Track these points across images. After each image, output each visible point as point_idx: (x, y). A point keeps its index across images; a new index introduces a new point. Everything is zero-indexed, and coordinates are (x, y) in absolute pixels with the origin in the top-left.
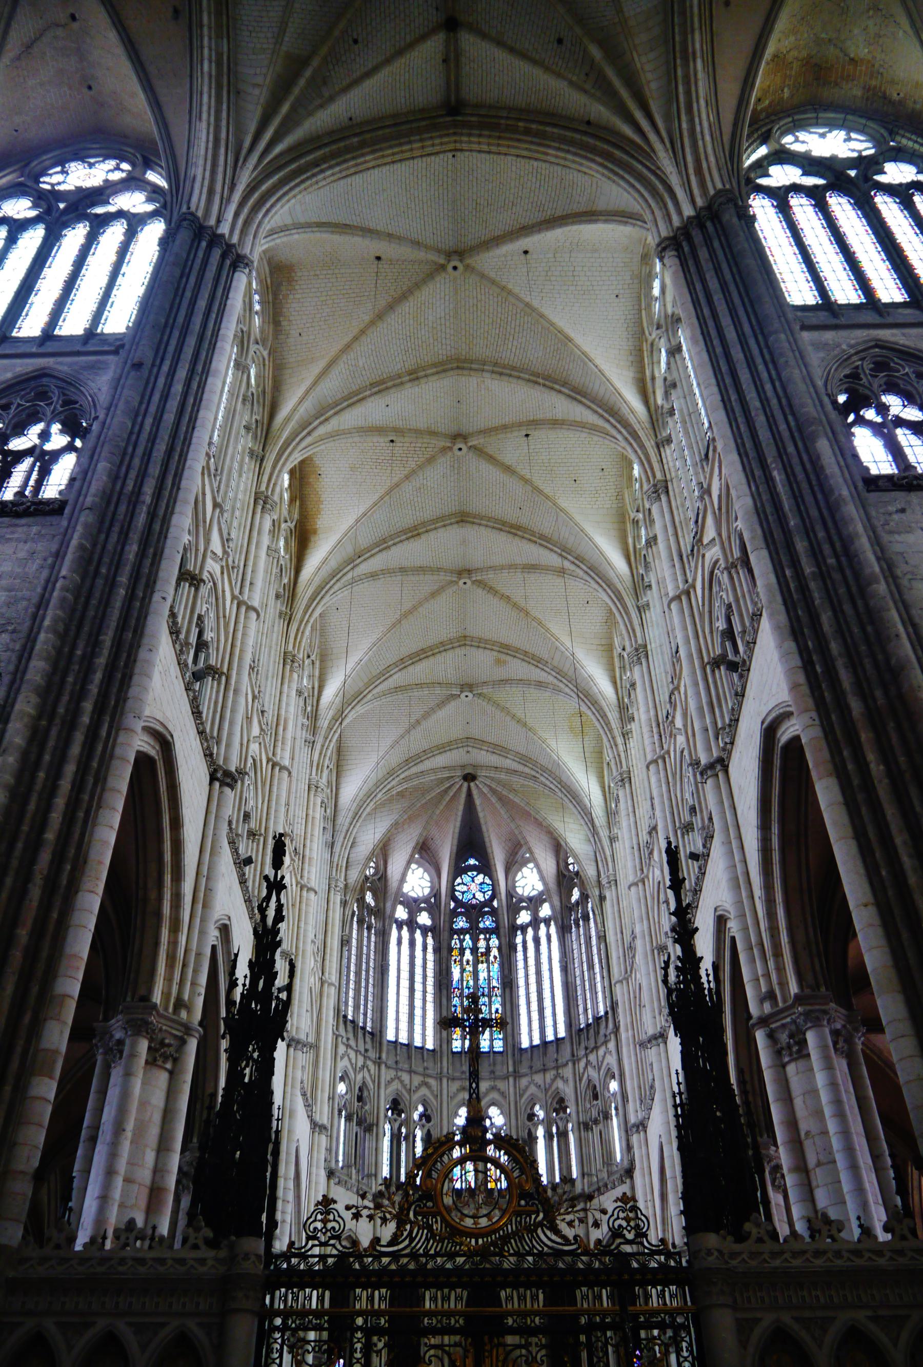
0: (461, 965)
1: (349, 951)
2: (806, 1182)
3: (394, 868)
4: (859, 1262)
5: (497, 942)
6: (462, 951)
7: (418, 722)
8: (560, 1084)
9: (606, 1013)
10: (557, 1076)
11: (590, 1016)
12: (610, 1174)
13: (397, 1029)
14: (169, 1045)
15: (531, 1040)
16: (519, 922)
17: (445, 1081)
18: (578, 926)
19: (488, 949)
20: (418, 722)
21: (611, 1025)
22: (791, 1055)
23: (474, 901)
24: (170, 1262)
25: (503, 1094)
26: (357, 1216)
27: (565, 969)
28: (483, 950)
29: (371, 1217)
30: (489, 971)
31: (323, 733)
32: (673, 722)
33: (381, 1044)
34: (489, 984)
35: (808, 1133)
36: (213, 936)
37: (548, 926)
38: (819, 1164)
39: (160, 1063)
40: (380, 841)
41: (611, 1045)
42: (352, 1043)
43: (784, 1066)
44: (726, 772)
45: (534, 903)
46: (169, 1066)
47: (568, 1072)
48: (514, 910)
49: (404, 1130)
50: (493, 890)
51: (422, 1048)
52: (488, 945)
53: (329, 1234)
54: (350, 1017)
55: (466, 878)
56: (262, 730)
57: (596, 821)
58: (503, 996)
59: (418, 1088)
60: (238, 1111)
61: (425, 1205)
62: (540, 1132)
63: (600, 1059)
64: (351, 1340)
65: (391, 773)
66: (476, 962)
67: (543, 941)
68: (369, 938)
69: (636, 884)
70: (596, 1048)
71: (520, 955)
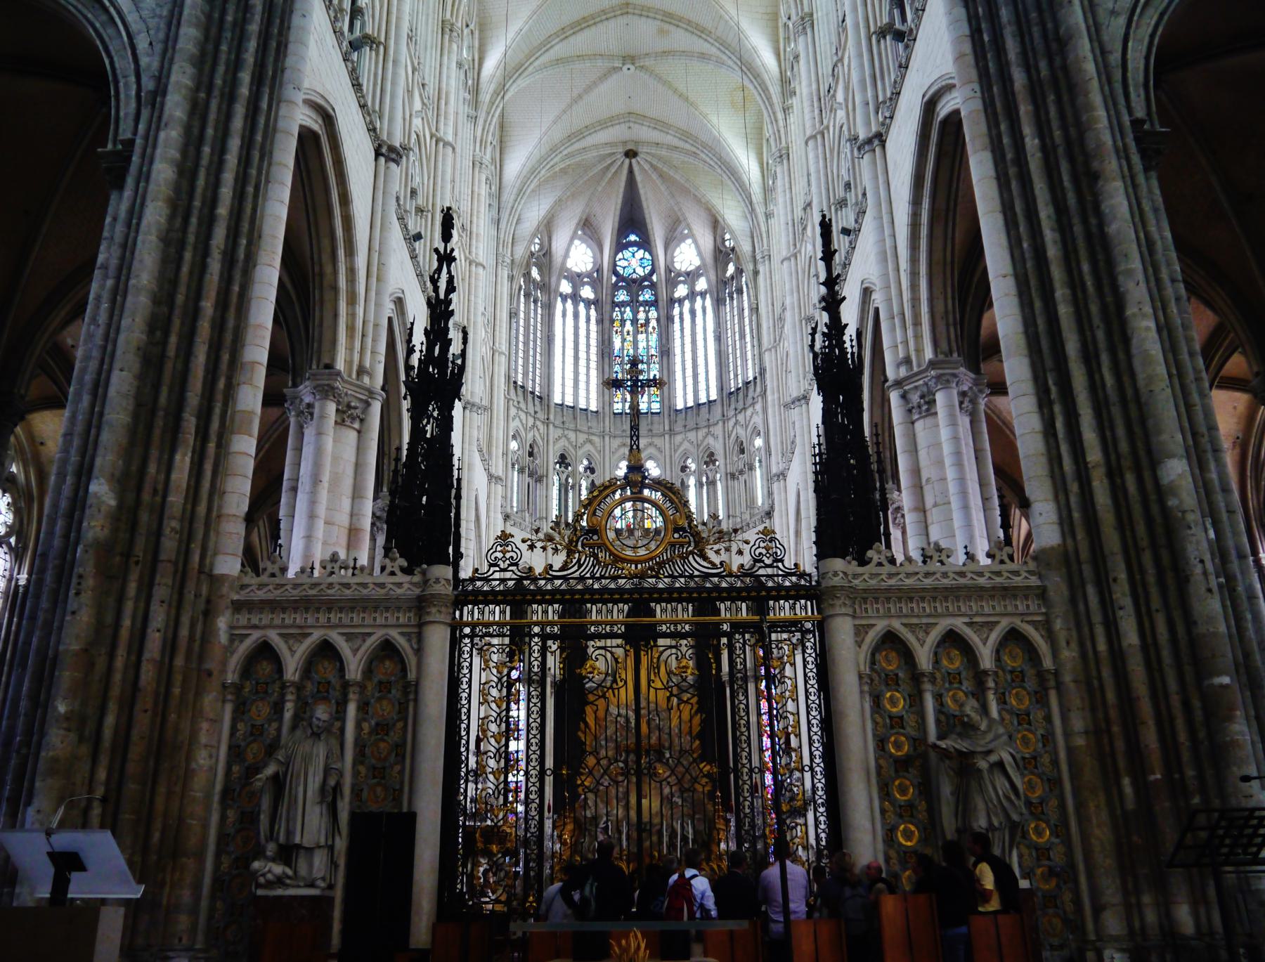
0: (622, 335)
1: (517, 322)
2: (923, 519)
3: (558, 245)
4: (962, 581)
5: (655, 314)
6: (623, 322)
7: (580, 97)
8: (710, 440)
9: (755, 378)
11: (740, 381)
12: (752, 516)
13: (563, 393)
14: (355, 408)
15: (686, 402)
16: (676, 295)
17: (607, 438)
18: (732, 299)
19: (647, 320)
20: (580, 97)
21: (758, 389)
22: (920, 413)
23: (634, 276)
24: (371, 586)
25: (659, 450)
26: (532, 547)
27: (719, 338)
28: (643, 322)
29: (544, 548)
30: (648, 341)
31: (485, 108)
32: (834, 96)
33: (548, 406)
34: (648, 352)
35: (928, 480)
36: (389, 309)
37: (704, 298)
38: (935, 505)
39: (348, 423)
40: (544, 218)
42: (523, 405)
43: (913, 423)
44: (884, 147)
45: (691, 276)
46: (356, 425)
47: (718, 430)
48: (672, 283)
49: (570, 480)
50: (653, 265)
51: (586, 410)
52: (647, 316)
53: (508, 562)
54: (520, 383)
55: (627, 254)
56: (423, 104)
57: (753, 197)
58: (661, 363)
59: (582, 445)
60: (422, 462)
61: (591, 538)
62: (692, 481)
63: (748, 418)
64: (530, 644)
65: (554, 150)
66: (636, 332)
68: (535, 311)
69: (788, 259)
70: (745, 409)
71: (677, 325)
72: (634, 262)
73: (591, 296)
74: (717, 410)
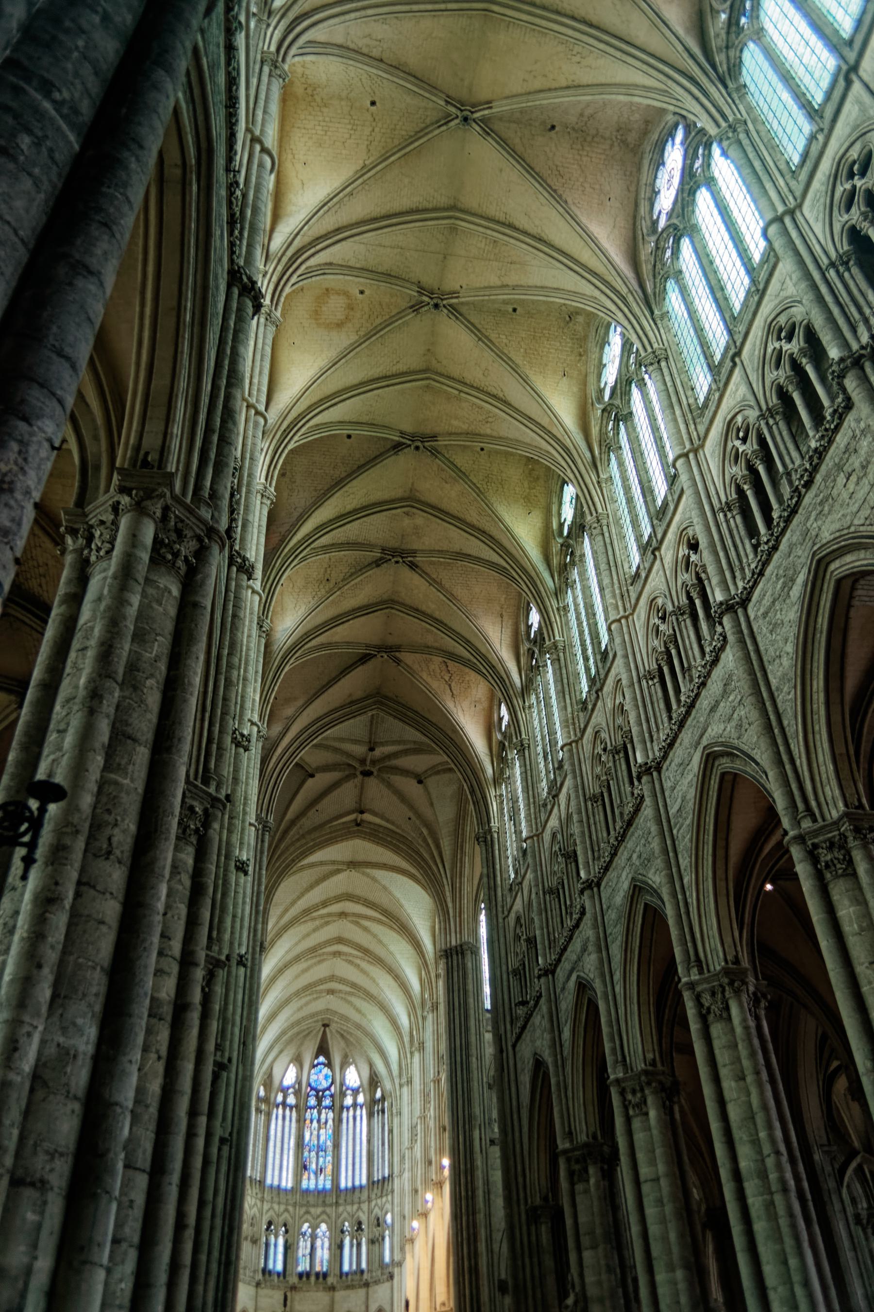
10: (359, 1208)
12: (382, 1274)
23: (320, 1087)
25: (329, 1217)
27: (369, 1141)
37: (361, 1107)
41: (390, 1197)
45: (356, 1092)
47: (365, 1207)
48: (343, 1095)
66: (319, 1128)
67: (358, 1118)
70: (381, 1197)
72: (321, 1077)
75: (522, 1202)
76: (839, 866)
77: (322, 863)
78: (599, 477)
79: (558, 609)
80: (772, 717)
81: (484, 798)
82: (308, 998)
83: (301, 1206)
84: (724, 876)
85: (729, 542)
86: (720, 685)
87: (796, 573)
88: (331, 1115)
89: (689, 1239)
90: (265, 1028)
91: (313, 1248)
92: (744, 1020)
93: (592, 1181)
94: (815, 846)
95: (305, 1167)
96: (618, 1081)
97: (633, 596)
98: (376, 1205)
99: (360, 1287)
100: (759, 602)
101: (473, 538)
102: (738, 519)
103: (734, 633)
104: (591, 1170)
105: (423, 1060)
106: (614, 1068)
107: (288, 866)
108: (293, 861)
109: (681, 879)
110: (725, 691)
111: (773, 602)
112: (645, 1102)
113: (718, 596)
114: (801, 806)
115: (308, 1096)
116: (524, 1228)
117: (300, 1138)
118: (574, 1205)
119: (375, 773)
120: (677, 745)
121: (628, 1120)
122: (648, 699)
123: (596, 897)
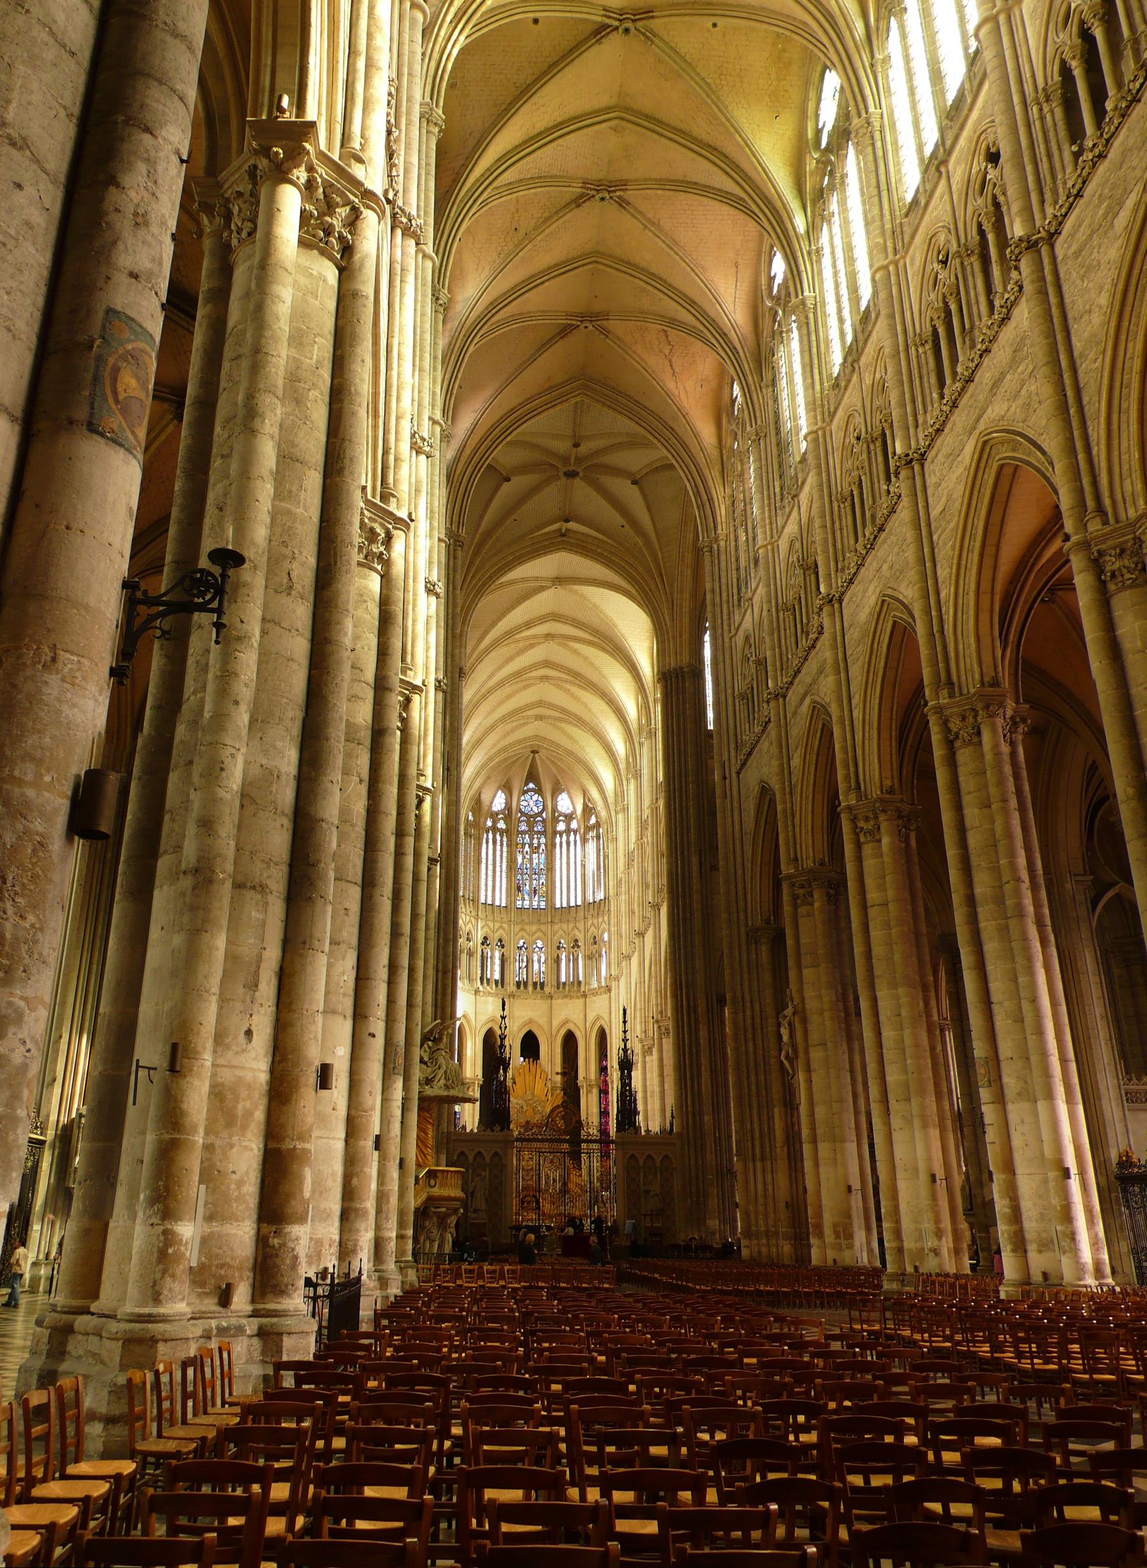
6: (523, 845)
8: (577, 932)
16: (558, 829)
19: (539, 844)
37: (575, 835)
41: (606, 918)
45: (569, 818)
47: (581, 925)
48: (555, 821)
55: (527, 797)
58: (547, 875)
62: (563, 957)
72: (531, 803)
73: (504, 827)
74: (581, 914)
75: (742, 923)
76: (1128, 576)
77: (523, 580)
78: (873, 57)
79: (809, 253)
80: (1070, 393)
81: (710, 500)
82: (515, 724)
83: (517, 923)
84: (989, 590)
85: (1041, 150)
86: (1009, 351)
87: (1127, 192)
88: (543, 840)
89: (915, 959)
90: (468, 758)
91: (529, 961)
92: (996, 746)
93: (817, 905)
94: (1101, 553)
95: (519, 889)
96: (850, 808)
97: (908, 230)
98: (593, 924)
99: (578, 998)
100: (1072, 235)
101: (700, 159)
102: (1059, 113)
103: (1033, 282)
104: (816, 896)
105: (639, 788)
106: (847, 795)
107: (484, 585)
108: (491, 577)
109: (938, 593)
110: (1013, 359)
111: (1091, 236)
112: (879, 829)
113: (1017, 229)
114: (1090, 503)
115: (520, 822)
116: (744, 948)
117: (512, 861)
118: (796, 926)
119: (581, 474)
120: (947, 430)
121: (858, 846)
122: (915, 372)
123: (837, 614)
